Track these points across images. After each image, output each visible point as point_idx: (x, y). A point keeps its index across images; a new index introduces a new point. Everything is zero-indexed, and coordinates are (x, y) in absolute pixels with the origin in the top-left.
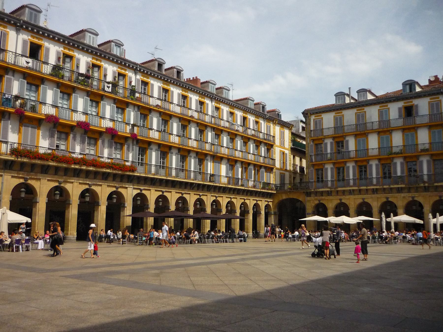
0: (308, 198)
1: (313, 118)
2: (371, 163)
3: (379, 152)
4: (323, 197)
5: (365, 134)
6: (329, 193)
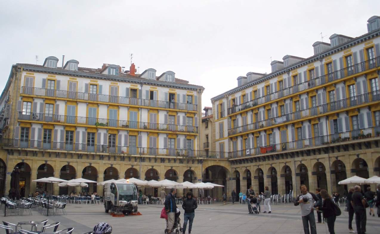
0: (11, 157)
1: (24, 74)
2: (78, 129)
3: (86, 120)
4: (28, 157)
5: (76, 102)
6: (34, 153)
